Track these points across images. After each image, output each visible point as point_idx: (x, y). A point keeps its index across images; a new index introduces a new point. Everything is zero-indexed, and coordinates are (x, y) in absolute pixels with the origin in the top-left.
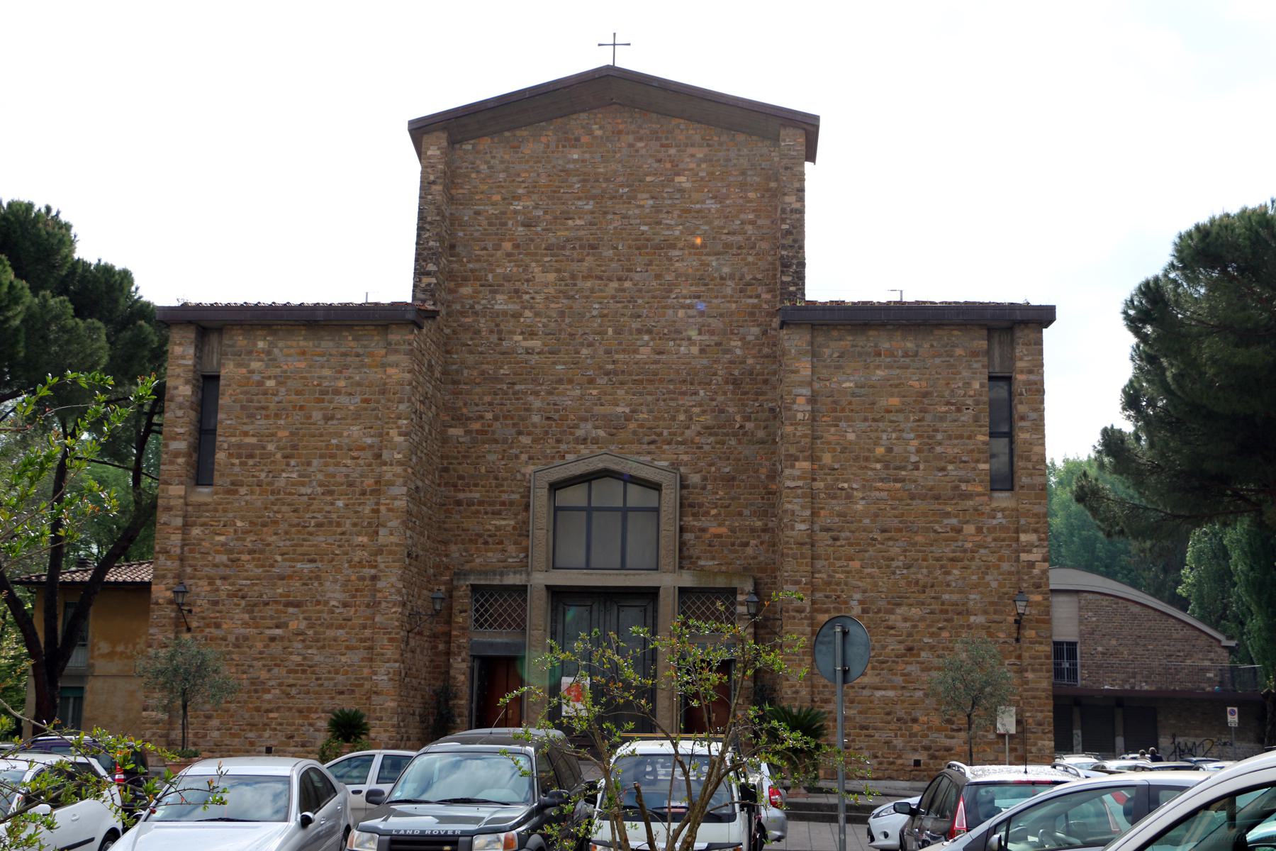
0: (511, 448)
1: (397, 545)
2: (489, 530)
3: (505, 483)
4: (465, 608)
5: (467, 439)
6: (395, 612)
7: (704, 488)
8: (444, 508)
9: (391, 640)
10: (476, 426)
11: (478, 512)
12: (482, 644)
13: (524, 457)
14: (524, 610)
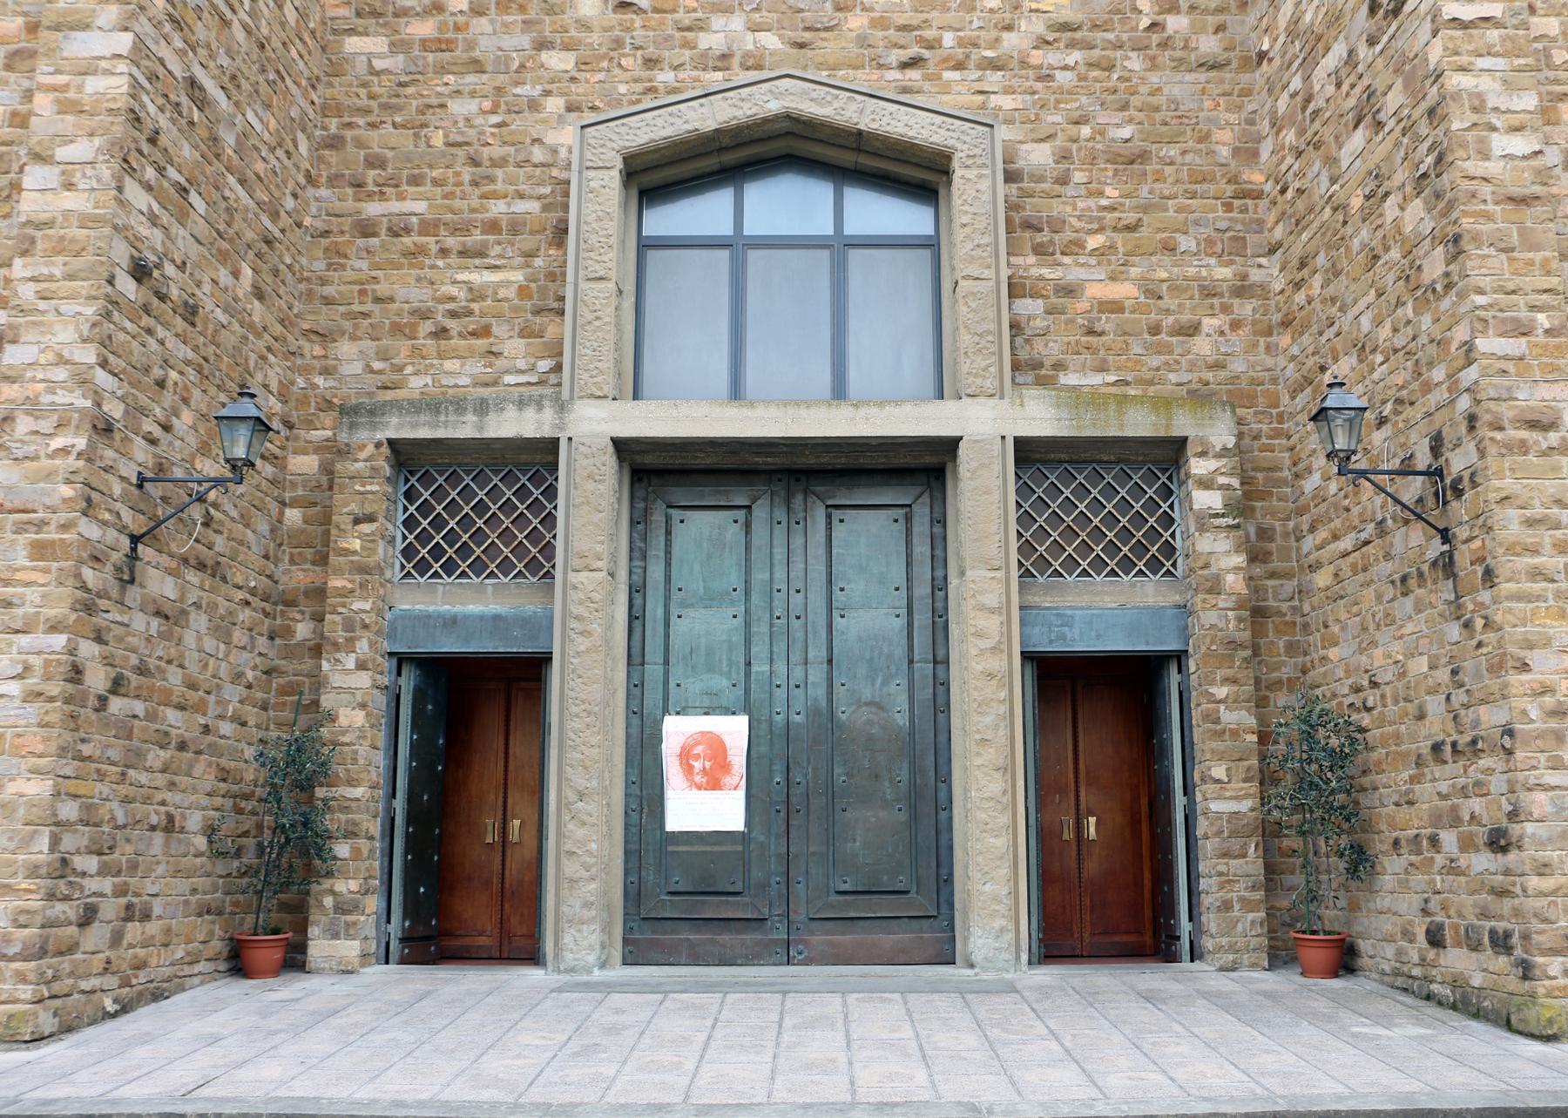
0: (517, 84)
1: (86, 221)
2: (452, 299)
3: (499, 173)
4: (368, 509)
5: (397, 62)
6: (65, 451)
7: (1063, 180)
8: (324, 242)
9: (40, 550)
10: (424, 28)
11: (421, 251)
12: (426, 618)
13: (554, 105)
14: (549, 520)
